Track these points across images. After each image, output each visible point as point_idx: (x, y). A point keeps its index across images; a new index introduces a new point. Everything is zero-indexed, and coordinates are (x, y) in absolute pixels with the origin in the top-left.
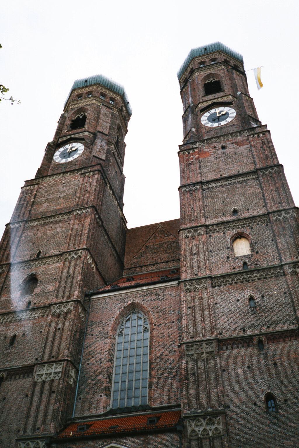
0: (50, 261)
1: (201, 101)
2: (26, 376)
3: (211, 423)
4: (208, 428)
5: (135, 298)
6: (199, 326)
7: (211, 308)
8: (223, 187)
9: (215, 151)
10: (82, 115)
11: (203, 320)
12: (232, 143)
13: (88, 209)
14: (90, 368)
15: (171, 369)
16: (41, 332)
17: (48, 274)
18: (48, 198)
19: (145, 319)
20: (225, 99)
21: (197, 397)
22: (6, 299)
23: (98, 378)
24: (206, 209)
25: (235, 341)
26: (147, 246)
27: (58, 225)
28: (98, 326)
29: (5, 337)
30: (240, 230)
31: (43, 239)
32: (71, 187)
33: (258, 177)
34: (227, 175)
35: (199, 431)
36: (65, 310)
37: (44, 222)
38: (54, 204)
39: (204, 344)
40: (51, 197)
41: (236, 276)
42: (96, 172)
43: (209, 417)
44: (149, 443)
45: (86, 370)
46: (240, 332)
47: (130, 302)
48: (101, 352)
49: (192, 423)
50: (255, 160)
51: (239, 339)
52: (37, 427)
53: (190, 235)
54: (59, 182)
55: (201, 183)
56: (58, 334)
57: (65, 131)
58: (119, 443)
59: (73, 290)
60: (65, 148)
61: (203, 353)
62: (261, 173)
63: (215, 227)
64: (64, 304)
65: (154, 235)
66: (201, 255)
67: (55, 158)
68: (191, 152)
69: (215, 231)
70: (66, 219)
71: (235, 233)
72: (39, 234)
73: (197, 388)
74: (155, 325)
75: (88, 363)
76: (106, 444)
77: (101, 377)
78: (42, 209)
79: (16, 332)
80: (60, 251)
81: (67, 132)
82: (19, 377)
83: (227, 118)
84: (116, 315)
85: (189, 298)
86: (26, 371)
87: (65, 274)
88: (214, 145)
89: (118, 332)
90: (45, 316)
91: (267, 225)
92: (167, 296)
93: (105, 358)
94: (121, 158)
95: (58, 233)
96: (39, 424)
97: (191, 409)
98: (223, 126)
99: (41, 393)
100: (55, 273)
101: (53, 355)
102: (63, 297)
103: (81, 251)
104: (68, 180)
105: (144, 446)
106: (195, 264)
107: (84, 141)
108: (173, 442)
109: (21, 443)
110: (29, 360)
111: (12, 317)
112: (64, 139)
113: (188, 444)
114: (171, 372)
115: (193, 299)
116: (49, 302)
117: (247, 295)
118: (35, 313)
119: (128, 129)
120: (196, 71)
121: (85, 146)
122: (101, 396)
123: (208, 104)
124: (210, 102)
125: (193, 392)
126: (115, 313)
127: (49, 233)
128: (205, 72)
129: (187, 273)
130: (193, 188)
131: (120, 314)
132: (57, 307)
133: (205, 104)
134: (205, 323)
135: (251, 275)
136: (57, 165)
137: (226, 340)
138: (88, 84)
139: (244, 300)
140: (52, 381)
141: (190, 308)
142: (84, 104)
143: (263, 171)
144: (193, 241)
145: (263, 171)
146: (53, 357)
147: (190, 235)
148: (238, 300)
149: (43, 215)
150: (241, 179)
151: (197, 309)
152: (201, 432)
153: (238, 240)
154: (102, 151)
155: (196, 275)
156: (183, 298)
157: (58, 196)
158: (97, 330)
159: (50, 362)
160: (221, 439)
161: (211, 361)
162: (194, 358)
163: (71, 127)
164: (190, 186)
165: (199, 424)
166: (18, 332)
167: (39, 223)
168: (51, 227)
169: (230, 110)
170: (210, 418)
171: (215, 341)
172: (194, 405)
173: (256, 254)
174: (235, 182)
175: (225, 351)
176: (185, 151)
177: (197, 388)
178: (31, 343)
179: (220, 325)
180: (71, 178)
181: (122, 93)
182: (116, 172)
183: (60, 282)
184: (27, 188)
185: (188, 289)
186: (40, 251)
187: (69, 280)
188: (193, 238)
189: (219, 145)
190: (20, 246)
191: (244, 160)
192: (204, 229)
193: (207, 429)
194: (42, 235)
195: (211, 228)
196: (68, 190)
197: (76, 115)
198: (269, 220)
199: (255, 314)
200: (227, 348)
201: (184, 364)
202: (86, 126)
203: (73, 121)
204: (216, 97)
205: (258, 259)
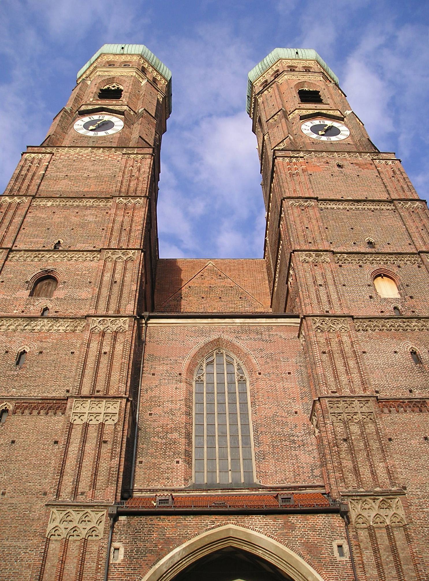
0: (79, 257)
1: (298, 107)
2: (49, 414)
3: (385, 507)
5: (223, 332)
6: (344, 378)
7: (359, 356)
8: (348, 211)
9: (328, 166)
10: (114, 87)
11: (348, 372)
12: (352, 164)
14: (155, 421)
15: (293, 436)
16: (72, 353)
17: (78, 275)
18: (68, 174)
19: (238, 365)
20: (331, 113)
21: (356, 471)
22: (4, 298)
23: (169, 436)
24: (327, 233)
25: (401, 404)
26: (190, 287)
27: (88, 212)
28: (164, 363)
29: (7, 352)
30: (382, 265)
31: (64, 226)
32: (106, 168)
33: (396, 209)
34: (351, 198)
37: (64, 203)
38: (79, 183)
39: (356, 401)
40: (74, 174)
41: (388, 322)
42: (148, 156)
43: (381, 498)
44: (293, 527)
45: (148, 423)
46: (405, 393)
47: (214, 336)
48: (172, 401)
50: (388, 188)
51: (406, 401)
52: (80, 490)
53: (311, 259)
54: (85, 157)
55: (316, 199)
56: (104, 360)
57: (91, 100)
58: (242, 523)
59: (123, 302)
61: (356, 413)
62: (400, 205)
63: (345, 257)
64: (112, 319)
65: (201, 274)
66: (332, 288)
67: (75, 127)
68: (294, 160)
69: (346, 262)
70: (101, 206)
71: (376, 269)
72: (57, 219)
73: (354, 460)
74: (260, 374)
75: (149, 412)
76: (219, 524)
77: (175, 435)
78: (58, 186)
79: (26, 346)
80: (94, 247)
81: (94, 101)
82: (39, 413)
84: (193, 352)
85: (322, 340)
86: (50, 405)
87: (107, 277)
88: (327, 161)
89: (195, 378)
90: (78, 331)
91: (419, 267)
92: (276, 337)
93: (180, 409)
95: (90, 222)
96: (84, 485)
97: (348, 487)
98: (335, 142)
99: (84, 441)
100: (90, 275)
101: (97, 389)
102: (108, 309)
103: (133, 251)
104: (101, 158)
106: (324, 298)
107: (124, 116)
108: (333, 528)
109: (54, 510)
110: (54, 391)
111: (17, 324)
112: (90, 107)
113: (355, 533)
114: (294, 440)
115: (328, 341)
116: (84, 312)
117: (407, 347)
118: (58, 325)
120: (286, 74)
121: (125, 123)
123: (308, 113)
124: (311, 112)
125: (348, 464)
126: (191, 349)
127: (74, 220)
128: (298, 78)
129: (313, 307)
130: (306, 204)
131: (198, 352)
132: (99, 322)
133: (304, 113)
134: (352, 375)
135: (409, 324)
136: (81, 137)
137: (387, 400)
139: (405, 352)
140: (103, 424)
141: (324, 353)
142: (119, 74)
143: (402, 203)
144: (316, 267)
145: (402, 203)
146: (98, 391)
147: (311, 259)
148: (395, 352)
149: (61, 195)
150: (372, 207)
151: (336, 355)
152: (372, 517)
153: (379, 278)
154: (148, 135)
155: (327, 312)
156: (314, 339)
157: (85, 175)
158: (160, 368)
159: (96, 397)
160: (405, 530)
161: (369, 425)
163: (99, 97)
164: (301, 200)
165: (367, 507)
166: (30, 348)
167: (54, 204)
168: (77, 213)
169: (340, 126)
171: (373, 399)
172: (352, 482)
173: (410, 299)
174: (364, 209)
175: (388, 415)
176: (286, 158)
177: (354, 460)
178: (55, 367)
179: (375, 381)
180: (106, 156)
183: (100, 289)
185: (319, 328)
186: (59, 242)
187: (116, 288)
188: (316, 264)
189: (334, 163)
190: (24, 229)
191: (372, 186)
192: (329, 254)
194: (62, 220)
195: (340, 256)
196: (102, 170)
198: (422, 260)
199: (423, 372)
200: (390, 411)
201: (328, 425)
203: (101, 90)
204: (318, 108)
205: (414, 305)
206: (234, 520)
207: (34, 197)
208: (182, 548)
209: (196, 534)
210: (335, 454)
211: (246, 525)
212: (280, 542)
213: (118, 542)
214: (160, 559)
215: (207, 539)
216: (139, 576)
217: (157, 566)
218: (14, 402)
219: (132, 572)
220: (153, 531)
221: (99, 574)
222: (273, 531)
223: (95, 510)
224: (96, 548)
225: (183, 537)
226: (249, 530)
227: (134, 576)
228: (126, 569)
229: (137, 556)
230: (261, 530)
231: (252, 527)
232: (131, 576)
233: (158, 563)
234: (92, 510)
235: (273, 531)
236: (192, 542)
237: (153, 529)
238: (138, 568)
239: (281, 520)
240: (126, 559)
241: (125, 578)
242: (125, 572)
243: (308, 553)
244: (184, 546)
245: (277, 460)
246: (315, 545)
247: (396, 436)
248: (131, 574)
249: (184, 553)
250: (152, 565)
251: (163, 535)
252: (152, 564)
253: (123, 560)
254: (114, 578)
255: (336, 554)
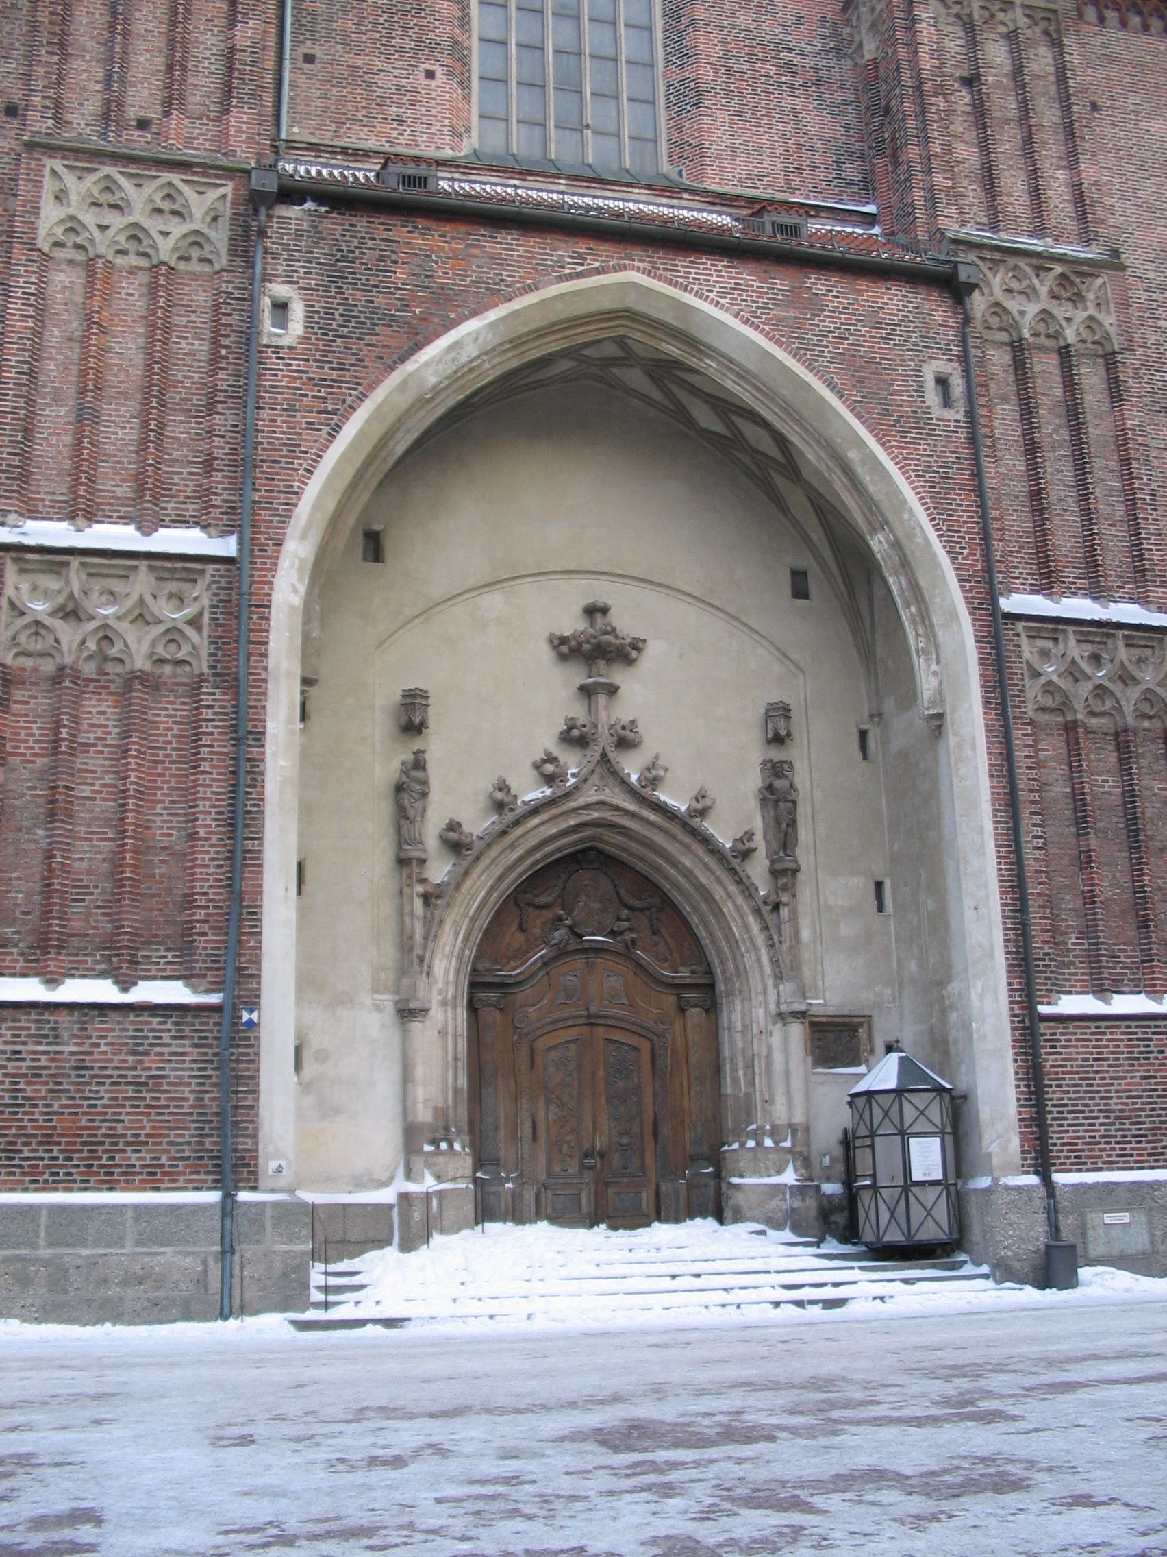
4: (1061, 311)
21: (989, 178)
35: (1022, 313)
43: (1059, 269)
44: (815, 306)
49: (989, 274)
76: (597, 264)
105: (792, 313)
114: (790, 63)
122: (430, 75)
162: (970, 15)
170: (1062, 276)
177: (985, 146)
193: (1055, 312)
206: (643, 261)
208: (486, 322)
209: (529, 286)
210: (936, 117)
211: (680, 280)
212: (778, 343)
213: (284, 282)
214: (418, 347)
215: (559, 306)
216: (355, 389)
217: (410, 366)
219: (334, 377)
220: (395, 262)
221: (222, 375)
222: (758, 307)
223: (195, 179)
224: (203, 298)
225: (488, 289)
226: (686, 294)
227: (340, 388)
228: (315, 364)
229: (346, 330)
230: (722, 301)
231: (696, 287)
232: (331, 387)
233: (413, 358)
234: (184, 177)
235: (758, 307)
236: (517, 307)
237: (394, 257)
238: (352, 365)
239: (781, 282)
240: (313, 337)
241: (312, 390)
242: (310, 375)
243: (854, 386)
244: (493, 315)
245: (739, 114)
246: (874, 366)
247: (1112, 98)
248: (333, 381)
249: (490, 336)
250: (395, 363)
251: (427, 276)
252: (395, 358)
253: (304, 339)
254: (276, 387)
255: (932, 397)
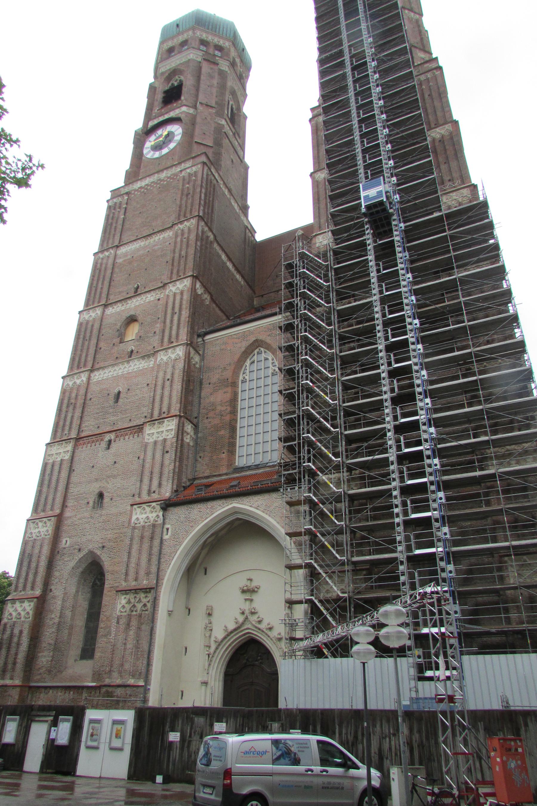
2: (135, 437)
13: (192, 220)
36: (173, 356)
60: (157, 135)
67: (145, 151)
77: (222, 432)
83: (174, 137)
94: (239, 137)
119: (248, 91)
138: (181, 30)
140: (165, 440)
146: (164, 413)
181: (232, 35)
182: (232, 161)
184: (115, 200)
186: (138, 285)
197: (169, 83)
202: (182, 98)
207: (117, 247)
218: (114, 433)
